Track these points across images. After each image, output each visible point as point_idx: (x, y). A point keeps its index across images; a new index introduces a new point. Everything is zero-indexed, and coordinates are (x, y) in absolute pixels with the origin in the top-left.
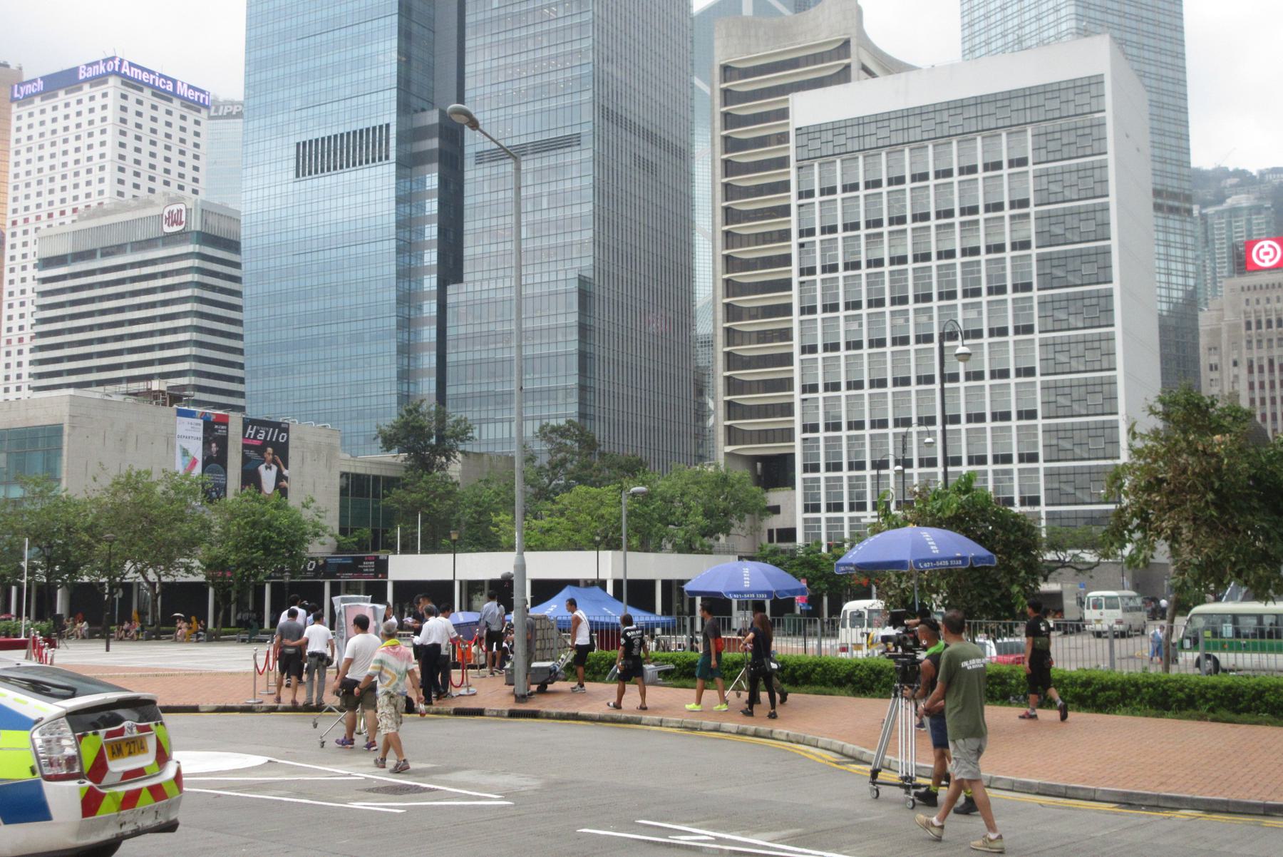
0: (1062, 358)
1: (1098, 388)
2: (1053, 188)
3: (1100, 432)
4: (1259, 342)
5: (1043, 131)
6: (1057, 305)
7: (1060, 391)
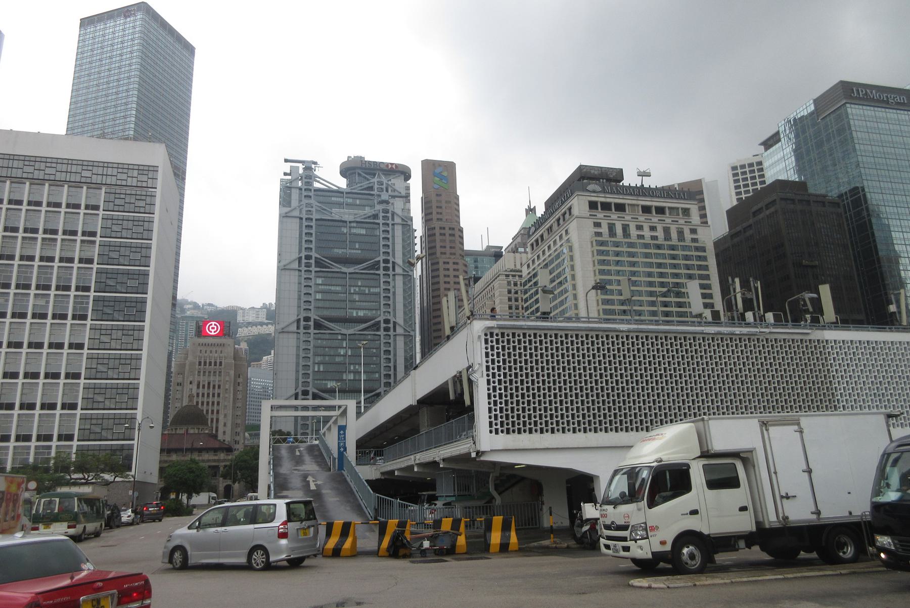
0: (105, 339)
1: (128, 362)
2: (115, 228)
3: (125, 391)
4: (204, 372)
5: (113, 191)
6: (106, 303)
7: (100, 361)
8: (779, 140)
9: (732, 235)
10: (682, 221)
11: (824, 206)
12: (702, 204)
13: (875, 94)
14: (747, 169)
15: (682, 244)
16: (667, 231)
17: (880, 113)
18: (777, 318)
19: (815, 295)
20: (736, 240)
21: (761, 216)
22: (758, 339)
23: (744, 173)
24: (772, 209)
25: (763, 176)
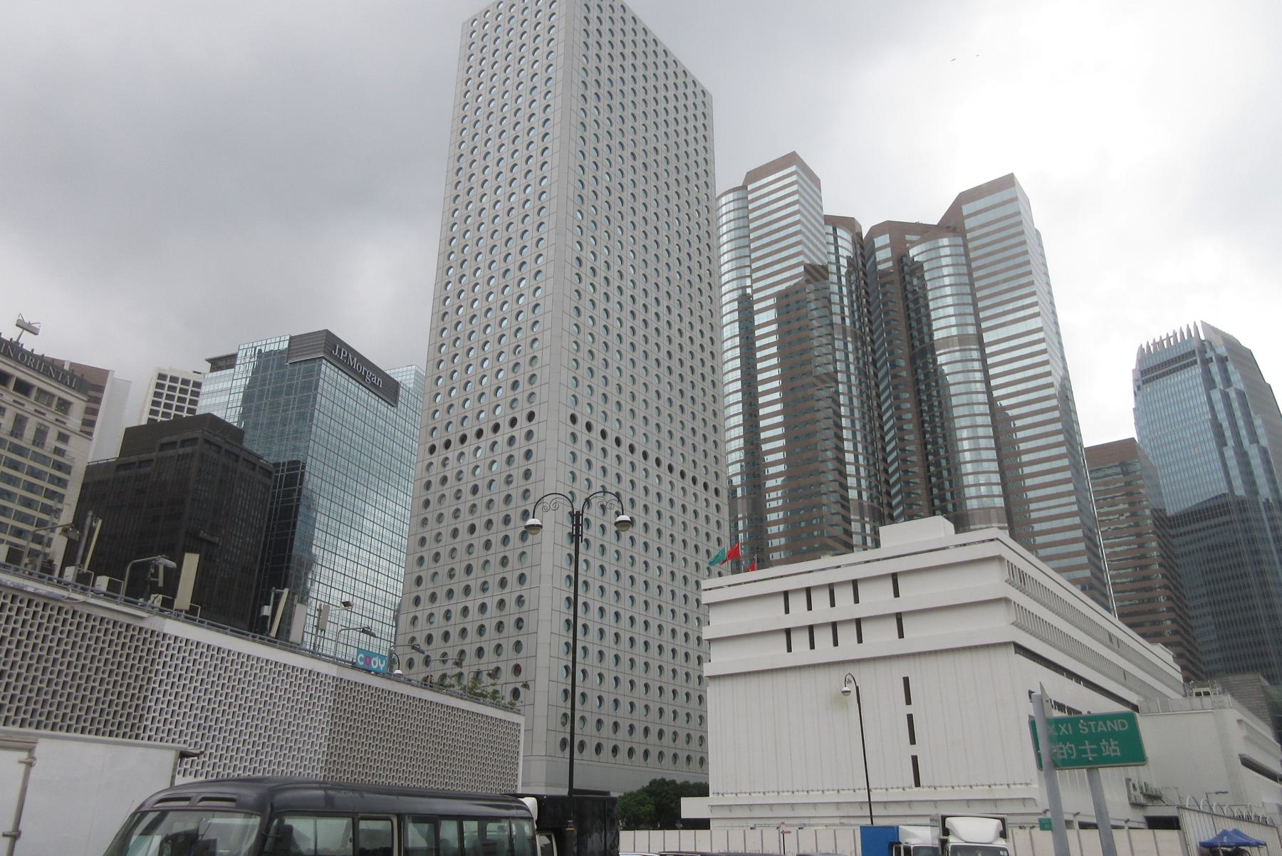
8: (232, 366)
9: (120, 465)
10: (50, 417)
11: (254, 469)
12: (93, 405)
13: (354, 362)
14: (179, 386)
15: (37, 450)
16: (20, 421)
17: (353, 386)
18: (113, 587)
19: (172, 564)
20: (122, 473)
21: (171, 452)
22: (60, 609)
23: (172, 388)
24: (188, 450)
25: (194, 402)
